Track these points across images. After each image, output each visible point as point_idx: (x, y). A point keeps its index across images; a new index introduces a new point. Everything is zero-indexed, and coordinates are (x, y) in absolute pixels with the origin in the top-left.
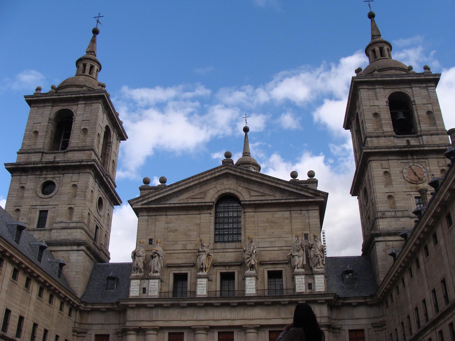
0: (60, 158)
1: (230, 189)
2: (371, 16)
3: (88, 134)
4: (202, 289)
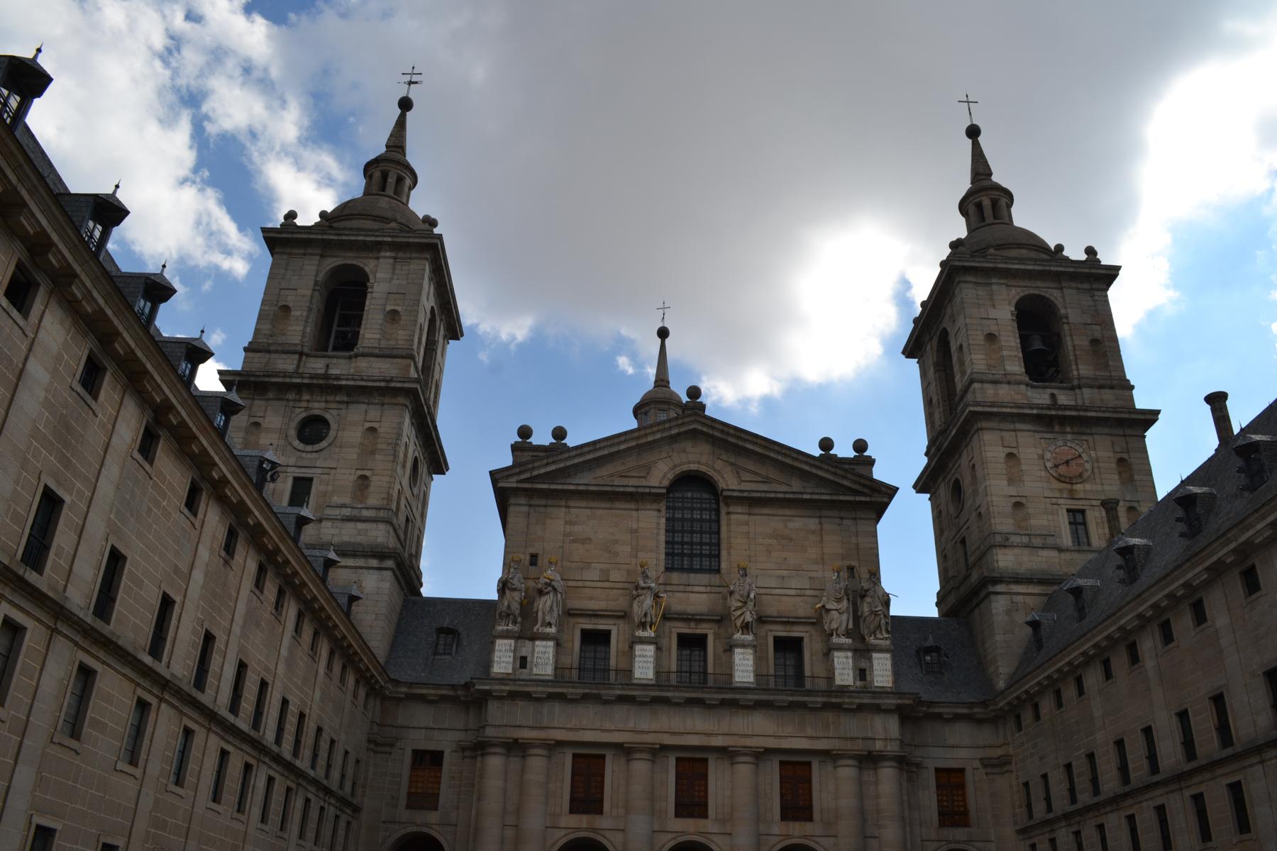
0: (340, 367)
1: (699, 463)
2: (973, 132)
3: (402, 323)
4: (644, 666)
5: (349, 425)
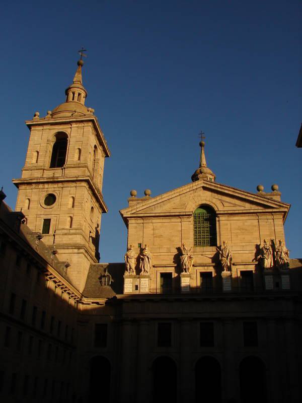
5: (65, 196)
